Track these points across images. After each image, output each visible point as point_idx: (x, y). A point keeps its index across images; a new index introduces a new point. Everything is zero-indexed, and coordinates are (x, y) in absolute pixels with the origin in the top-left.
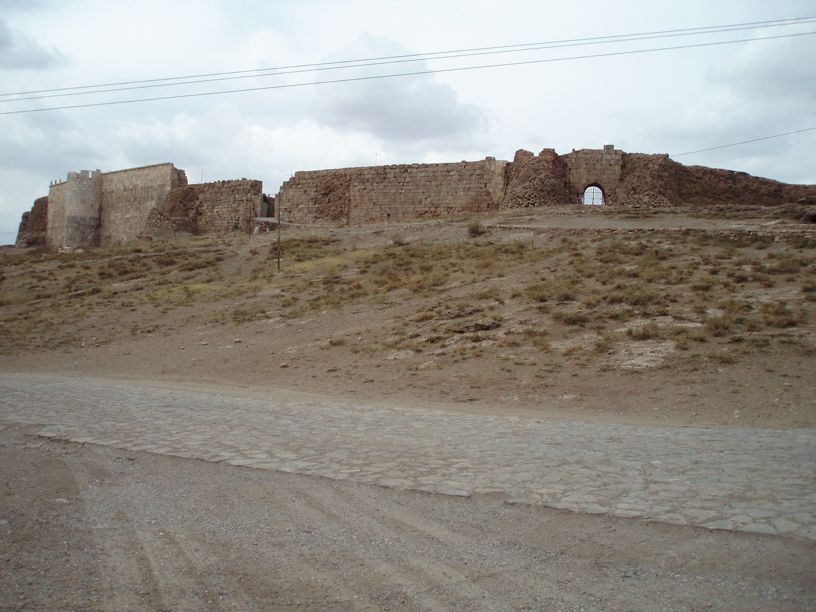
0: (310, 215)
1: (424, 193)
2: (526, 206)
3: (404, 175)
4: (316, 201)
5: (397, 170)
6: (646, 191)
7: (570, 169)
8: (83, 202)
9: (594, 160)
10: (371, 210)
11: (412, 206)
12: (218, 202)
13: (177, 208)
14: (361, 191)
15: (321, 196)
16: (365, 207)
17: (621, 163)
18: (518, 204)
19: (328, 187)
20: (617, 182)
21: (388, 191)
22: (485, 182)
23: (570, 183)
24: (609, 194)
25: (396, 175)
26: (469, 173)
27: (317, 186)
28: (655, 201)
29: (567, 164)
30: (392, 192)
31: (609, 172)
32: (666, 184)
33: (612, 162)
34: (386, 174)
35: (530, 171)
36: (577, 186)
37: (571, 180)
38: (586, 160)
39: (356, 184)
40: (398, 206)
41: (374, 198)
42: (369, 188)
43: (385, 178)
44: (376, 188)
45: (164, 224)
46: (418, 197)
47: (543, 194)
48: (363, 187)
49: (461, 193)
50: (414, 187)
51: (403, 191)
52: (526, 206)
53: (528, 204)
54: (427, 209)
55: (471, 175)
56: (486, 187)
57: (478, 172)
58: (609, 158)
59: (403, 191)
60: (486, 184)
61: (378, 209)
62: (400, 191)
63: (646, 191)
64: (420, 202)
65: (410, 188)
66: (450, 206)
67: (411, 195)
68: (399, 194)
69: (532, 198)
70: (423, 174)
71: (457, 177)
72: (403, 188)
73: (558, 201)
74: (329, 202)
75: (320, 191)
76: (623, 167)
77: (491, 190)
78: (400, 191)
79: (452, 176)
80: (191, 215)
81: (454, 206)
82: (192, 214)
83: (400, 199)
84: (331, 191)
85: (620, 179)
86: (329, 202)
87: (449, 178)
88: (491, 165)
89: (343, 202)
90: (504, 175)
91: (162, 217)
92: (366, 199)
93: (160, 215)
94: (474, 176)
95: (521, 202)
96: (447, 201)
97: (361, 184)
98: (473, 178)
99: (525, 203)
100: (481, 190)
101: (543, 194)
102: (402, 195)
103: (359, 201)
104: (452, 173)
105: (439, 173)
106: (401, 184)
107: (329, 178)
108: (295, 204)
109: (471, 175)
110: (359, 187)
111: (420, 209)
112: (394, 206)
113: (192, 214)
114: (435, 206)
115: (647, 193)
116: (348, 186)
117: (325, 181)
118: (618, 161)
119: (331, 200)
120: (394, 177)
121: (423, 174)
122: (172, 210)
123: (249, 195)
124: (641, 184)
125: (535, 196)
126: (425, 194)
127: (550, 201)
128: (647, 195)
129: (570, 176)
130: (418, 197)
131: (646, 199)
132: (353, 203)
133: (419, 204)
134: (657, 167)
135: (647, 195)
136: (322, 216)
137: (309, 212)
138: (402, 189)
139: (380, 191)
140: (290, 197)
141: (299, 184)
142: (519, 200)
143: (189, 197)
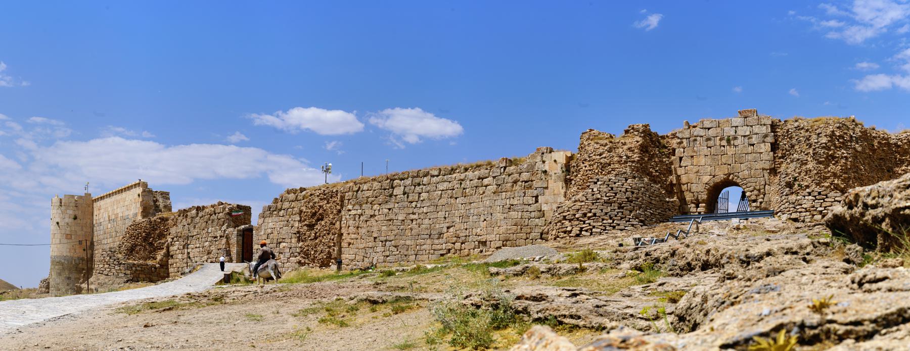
0: (294, 258)
1: (445, 218)
2: (578, 235)
3: (418, 189)
4: (300, 237)
5: (408, 182)
6: (807, 187)
7: (681, 159)
8: (68, 236)
9: (721, 140)
10: (371, 251)
11: (429, 241)
12: (190, 238)
13: (138, 248)
14: (357, 219)
15: (305, 228)
16: (362, 246)
17: (770, 139)
18: (565, 232)
19: (316, 212)
20: (766, 175)
21: (393, 217)
22: (535, 193)
23: (679, 184)
24: (753, 197)
25: (406, 190)
26: (510, 179)
27: (301, 211)
28: (824, 205)
29: (674, 150)
30: (400, 218)
31: (750, 157)
32: (845, 170)
33: (754, 140)
34: (393, 188)
35: (595, 166)
36: (694, 188)
37: (684, 179)
38: (708, 139)
39: (350, 207)
40: (408, 242)
41: (375, 229)
42: (369, 212)
43: (391, 196)
44: (377, 213)
45: (113, 271)
46: (437, 226)
47: (609, 209)
48: (359, 212)
49: (498, 216)
50: (432, 209)
51: (416, 217)
52: (578, 235)
53: (581, 230)
54: (450, 246)
55: (515, 182)
56: (537, 201)
57: (525, 176)
58: (748, 133)
59: (416, 217)
60: (537, 197)
61: (380, 249)
62: (412, 217)
63: (807, 187)
64: (440, 235)
65: (425, 210)
66: (483, 238)
67: (426, 221)
68: (409, 221)
69: (589, 218)
70: (445, 185)
71: (493, 188)
72: (415, 211)
73: (641, 221)
74: (316, 238)
75: (305, 220)
76: (774, 147)
77: (545, 208)
78: (412, 217)
79: (486, 186)
80: (159, 257)
81: (489, 238)
82: (160, 256)
83: (411, 229)
84: (318, 220)
85: (770, 169)
86: (316, 238)
87: (481, 190)
88: (544, 162)
89: (332, 237)
90: (563, 178)
91: (111, 260)
92: (363, 231)
93: (108, 258)
94: (520, 183)
95: (569, 229)
96: (478, 230)
97: (357, 207)
98: (517, 187)
99: (576, 231)
100: (530, 209)
101: (609, 209)
102: (414, 222)
103: (353, 236)
104: (486, 181)
105: (468, 182)
106: (414, 204)
107: (316, 200)
108: (275, 241)
109: (515, 182)
110: (353, 212)
111: (439, 247)
112: (402, 242)
113: (160, 256)
114: (461, 241)
115: (808, 190)
116: (339, 211)
117: (311, 204)
118: (766, 136)
119: (318, 234)
120: (404, 194)
121: (445, 185)
122: (131, 251)
123: (224, 227)
124: (800, 173)
125: (595, 215)
126: (447, 220)
127: (623, 222)
128: (810, 194)
129: (680, 171)
130: (437, 226)
131: (807, 203)
132: (346, 238)
133: (438, 238)
134: (824, 140)
135: (810, 194)
136: (307, 261)
137: (292, 255)
138: (414, 213)
139: (382, 217)
140: (269, 231)
141: (280, 210)
142: (567, 223)
143: (157, 232)
